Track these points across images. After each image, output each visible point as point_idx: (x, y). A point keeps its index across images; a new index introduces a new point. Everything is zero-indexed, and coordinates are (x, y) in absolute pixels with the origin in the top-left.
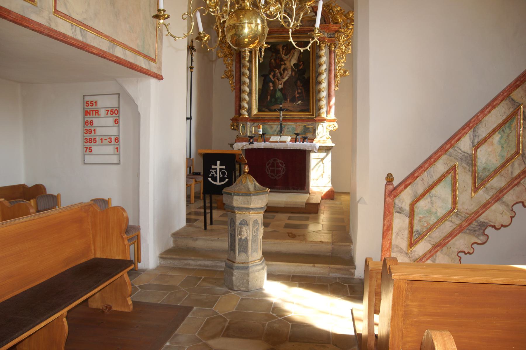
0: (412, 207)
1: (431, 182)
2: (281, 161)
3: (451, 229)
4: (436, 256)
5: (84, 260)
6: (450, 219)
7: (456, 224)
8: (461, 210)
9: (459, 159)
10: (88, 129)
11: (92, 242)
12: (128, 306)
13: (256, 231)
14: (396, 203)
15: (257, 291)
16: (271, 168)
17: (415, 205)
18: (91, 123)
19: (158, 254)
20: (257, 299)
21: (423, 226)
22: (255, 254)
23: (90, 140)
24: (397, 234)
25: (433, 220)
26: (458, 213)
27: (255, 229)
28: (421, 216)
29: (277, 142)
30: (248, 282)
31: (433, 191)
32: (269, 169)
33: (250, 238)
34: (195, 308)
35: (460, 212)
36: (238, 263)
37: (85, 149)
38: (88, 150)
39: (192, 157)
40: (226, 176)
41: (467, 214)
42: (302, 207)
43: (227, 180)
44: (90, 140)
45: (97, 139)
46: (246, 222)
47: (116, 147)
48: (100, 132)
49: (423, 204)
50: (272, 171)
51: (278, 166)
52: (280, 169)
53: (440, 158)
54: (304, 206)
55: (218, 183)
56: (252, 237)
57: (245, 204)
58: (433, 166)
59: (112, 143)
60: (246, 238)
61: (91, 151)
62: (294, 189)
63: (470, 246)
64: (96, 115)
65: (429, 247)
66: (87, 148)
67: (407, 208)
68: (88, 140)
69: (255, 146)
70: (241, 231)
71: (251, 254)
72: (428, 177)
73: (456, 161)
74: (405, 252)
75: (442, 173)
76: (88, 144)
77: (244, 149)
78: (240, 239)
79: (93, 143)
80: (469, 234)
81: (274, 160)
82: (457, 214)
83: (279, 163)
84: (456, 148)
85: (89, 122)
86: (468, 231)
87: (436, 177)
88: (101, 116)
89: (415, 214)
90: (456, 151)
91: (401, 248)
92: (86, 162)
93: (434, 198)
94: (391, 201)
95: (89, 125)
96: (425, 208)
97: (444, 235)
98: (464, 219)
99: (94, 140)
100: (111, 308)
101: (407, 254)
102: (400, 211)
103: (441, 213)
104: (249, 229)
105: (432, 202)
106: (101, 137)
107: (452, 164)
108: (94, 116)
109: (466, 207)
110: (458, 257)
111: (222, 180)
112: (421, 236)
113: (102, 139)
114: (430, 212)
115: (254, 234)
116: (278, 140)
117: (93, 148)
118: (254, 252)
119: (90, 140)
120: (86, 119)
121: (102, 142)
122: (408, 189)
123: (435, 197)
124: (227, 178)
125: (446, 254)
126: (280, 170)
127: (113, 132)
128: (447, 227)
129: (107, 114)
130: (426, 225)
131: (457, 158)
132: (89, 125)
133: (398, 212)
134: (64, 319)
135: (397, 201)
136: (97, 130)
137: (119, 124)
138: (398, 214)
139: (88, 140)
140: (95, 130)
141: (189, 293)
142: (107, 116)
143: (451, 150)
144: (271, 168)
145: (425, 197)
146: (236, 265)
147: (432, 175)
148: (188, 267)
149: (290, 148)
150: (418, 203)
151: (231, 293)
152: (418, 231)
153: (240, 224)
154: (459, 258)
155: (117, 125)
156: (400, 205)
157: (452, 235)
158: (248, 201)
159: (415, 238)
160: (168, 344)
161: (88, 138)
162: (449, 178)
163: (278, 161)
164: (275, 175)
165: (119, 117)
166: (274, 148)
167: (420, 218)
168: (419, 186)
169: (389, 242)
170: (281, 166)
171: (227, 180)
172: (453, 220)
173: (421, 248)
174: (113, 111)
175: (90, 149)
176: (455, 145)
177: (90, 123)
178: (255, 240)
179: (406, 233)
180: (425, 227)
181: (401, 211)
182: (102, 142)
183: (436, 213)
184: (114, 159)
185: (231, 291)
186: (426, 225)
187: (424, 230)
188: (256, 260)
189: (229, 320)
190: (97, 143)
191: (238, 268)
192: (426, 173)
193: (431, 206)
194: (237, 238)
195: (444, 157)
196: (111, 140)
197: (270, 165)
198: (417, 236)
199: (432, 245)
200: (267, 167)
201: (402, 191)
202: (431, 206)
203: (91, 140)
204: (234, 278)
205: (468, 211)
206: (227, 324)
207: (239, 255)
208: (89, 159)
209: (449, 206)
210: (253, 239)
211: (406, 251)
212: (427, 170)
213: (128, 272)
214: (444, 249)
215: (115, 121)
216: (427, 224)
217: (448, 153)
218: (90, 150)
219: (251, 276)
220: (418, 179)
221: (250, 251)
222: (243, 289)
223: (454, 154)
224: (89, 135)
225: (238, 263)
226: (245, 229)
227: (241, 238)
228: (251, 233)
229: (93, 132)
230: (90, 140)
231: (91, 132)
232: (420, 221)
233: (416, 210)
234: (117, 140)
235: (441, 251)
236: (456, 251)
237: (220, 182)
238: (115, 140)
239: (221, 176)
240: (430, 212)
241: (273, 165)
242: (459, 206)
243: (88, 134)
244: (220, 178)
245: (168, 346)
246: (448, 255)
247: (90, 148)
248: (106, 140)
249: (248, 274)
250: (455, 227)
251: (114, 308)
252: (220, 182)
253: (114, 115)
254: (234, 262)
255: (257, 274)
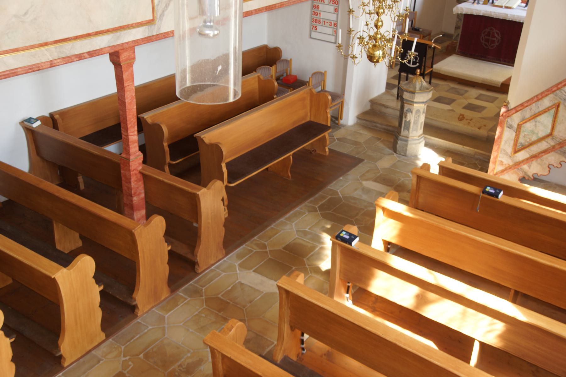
0: (519, 126)
1: (537, 111)
2: (497, 31)
3: (546, 148)
4: (532, 163)
5: (303, 122)
6: (547, 141)
7: (551, 145)
8: (556, 136)
9: (563, 99)
10: (315, 11)
11: (309, 111)
12: (326, 152)
13: (417, 117)
14: (508, 121)
15: (413, 157)
16: (486, 37)
17: (523, 125)
18: (318, 7)
19: (356, 114)
20: (408, 162)
21: (526, 141)
22: (415, 133)
23: (316, 21)
24: (506, 142)
25: (534, 138)
26: (554, 137)
27: (417, 116)
28: (526, 134)
29: (501, 7)
30: (406, 150)
31: (538, 118)
32: (484, 38)
33: (412, 121)
34: (365, 161)
35: (555, 137)
36: (402, 136)
37: (312, 27)
38: (314, 28)
39: (415, 10)
40: (418, 61)
41: (561, 139)
42: (497, 86)
43: (418, 64)
44: (316, 21)
45: (321, 21)
46: (411, 110)
47: (334, 30)
48: (323, 16)
49: (529, 126)
50: (487, 40)
51: (493, 36)
52: (495, 39)
53: (548, 96)
54: (499, 86)
55: (411, 65)
56: (414, 121)
57: (411, 98)
58: (541, 101)
59: (332, 26)
60: (409, 121)
61: (316, 30)
62: (505, 61)
63: (559, 162)
64: (321, 2)
65: (527, 156)
66: (313, 26)
67: (515, 126)
68: (315, 21)
69: (474, 12)
70: (406, 115)
71: (412, 132)
72: (535, 108)
73: (560, 100)
74: (509, 155)
75: (547, 107)
76: (314, 23)
77: (463, 14)
78: (406, 121)
79: (318, 24)
80: (560, 154)
81: (491, 29)
82: (553, 139)
83: (495, 33)
84: (562, 91)
85: (316, 6)
86: (559, 152)
87: (541, 109)
88: (326, 3)
89: (522, 131)
90: (562, 92)
91: (507, 152)
92: (312, 36)
93: (537, 123)
94: (503, 119)
95: (316, 9)
96: (530, 129)
97: (539, 150)
98: (557, 142)
99: (319, 21)
100: (316, 151)
101: (510, 157)
102: (510, 127)
103: (541, 134)
104: (412, 115)
105: (535, 126)
106: (324, 20)
107: (556, 102)
108: (320, 2)
109: (561, 135)
110: (547, 168)
111: (414, 63)
112: (524, 148)
113: (324, 22)
114: (533, 132)
115: (415, 119)
116: (503, 5)
117: (318, 27)
118: (414, 131)
119: (316, 20)
120: (314, 4)
121: (325, 24)
122: (518, 113)
123: (539, 122)
124: (418, 63)
125: (539, 164)
126: (495, 41)
127: (333, 17)
128: (544, 145)
129: (330, 3)
130: (528, 140)
131: (562, 98)
132: (316, 9)
133: (509, 128)
134: (291, 157)
135: (509, 119)
136: (322, 13)
137: (339, 5)
138: (508, 129)
139: (315, 21)
140: (320, 14)
141: (366, 149)
142: (329, 4)
143: (558, 92)
144: (486, 37)
145: (531, 121)
146: (400, 137)
147: (539, 107)
148: (375, 128)
149: (510, 19)
150: (525, 124)
151: (394, 154)
152: (522, 143)
153: (406, 111)
154: (548, 169)
155: (337, 13)
156: (511, 123)
157: (546, 152)
158: (413, 97)
159: (519, 147)
160: (341, 178)
161: (315, 19)
162: (553, 111)
163: (495, 31)
164: (489, 45)
165: (338, 7)
166: (493, 17)
167: (525, 134)
168: (527, 113)
169: (498, 146)
170: (497, 36)
171: (418, 64)
172: (549, 141)
173: (522, 155)
174: (335, 1)
175: (315, 28)
176: (562, 88)
177: (317, 7)
178: (416, 123)
179: (512, 143)
180: (527, 142)
181: (510, 127)
182: (325, 24)
183: (538, 134)
184: (332, 39)
185: (394, 153)
186: (528, 140)
187: (526, 144)
188: (415, 136)
189: (381, 172)
190: (321, 24)
191: (401, 140)
192: (534, 104)
193: (534, 128)
194: (404, 120)
195: (551, 96)
196: (331, 24)
197: (486, 33)
198: (520, 146)
199: (530, 155)
200: (483, 35)
201: (513, 114)
202: (534, 128)
203: (317, 21)
204: (398, 146)
205: (562, 138)
206: (379, 174)
207: (403, 131)
208: (314, 35)
209: (549, 131)
210: (414, 122)
211: (510, 155)
212: (536, 103)
213: (328, 133)
214: (539, 160)
215: (335, 10)
216: (530, 140)
217: (555, 93)
218: (316, 29)
219: (409, 147)
220: (527, 108)
221: (411, 130)
222: (402, 154)
223: (560, 94)
224: (316, 16)
225: (402, 136)
226: (409, 115)
227: (406, 120)
228: (413, 118)
229: (319, 15)
230: (316, 21)
231: (317, 14)
232: (524, 137)
233: (522, 129)
234: (336, 25)
235: (537, 161)
236: (547, 163)
237: (413, 64)
238: (334, 24)
239: (414, 60)
240: (533, 132)
241: (488, 35)
242: (555, 133)
243: (315, 16)
244: (413, 62)
245: (341, 180)
246: (541, 165)
247: (316, 27)
248: (327, 23)
249: (407, 145)
250: (549, 146)
251: (318, 152)
252: (413, 64)
253: (335, 5)
254: (400, 135)
255: (414, 146)
